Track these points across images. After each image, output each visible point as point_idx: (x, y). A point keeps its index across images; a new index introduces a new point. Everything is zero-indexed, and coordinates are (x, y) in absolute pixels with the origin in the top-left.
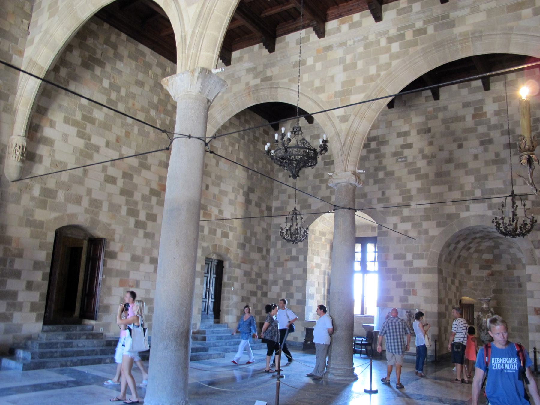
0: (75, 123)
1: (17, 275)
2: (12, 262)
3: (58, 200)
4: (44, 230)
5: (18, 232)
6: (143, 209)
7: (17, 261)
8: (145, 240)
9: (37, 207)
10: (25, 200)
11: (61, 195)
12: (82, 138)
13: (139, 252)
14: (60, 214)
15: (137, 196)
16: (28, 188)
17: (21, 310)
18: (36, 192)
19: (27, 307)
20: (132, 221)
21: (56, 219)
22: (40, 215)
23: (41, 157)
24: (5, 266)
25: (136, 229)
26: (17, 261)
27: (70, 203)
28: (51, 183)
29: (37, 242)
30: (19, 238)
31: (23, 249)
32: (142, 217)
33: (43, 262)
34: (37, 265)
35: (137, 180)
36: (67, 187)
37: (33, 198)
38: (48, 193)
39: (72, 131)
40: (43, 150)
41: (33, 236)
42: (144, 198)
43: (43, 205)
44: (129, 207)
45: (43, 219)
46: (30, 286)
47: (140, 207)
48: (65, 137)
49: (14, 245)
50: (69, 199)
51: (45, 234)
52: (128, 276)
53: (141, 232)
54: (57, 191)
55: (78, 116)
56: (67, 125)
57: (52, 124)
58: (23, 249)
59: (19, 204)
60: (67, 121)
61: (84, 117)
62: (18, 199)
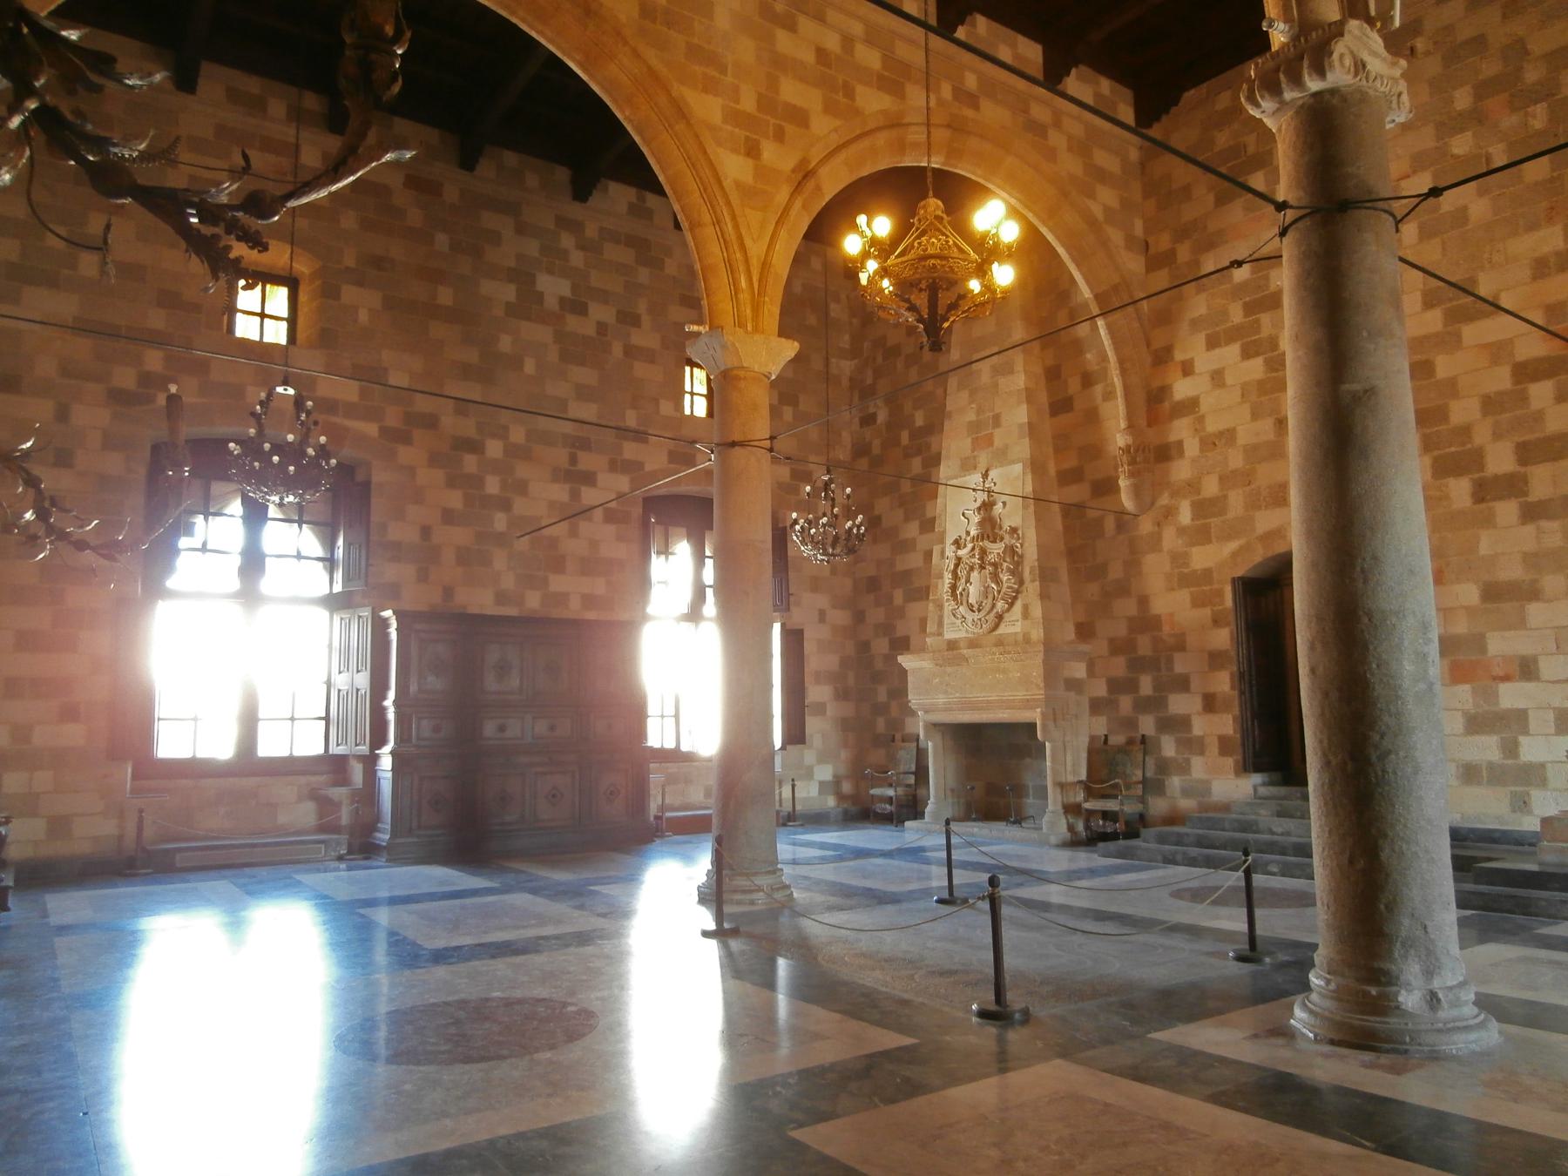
0: (1233, 335)
1: (1183, 684)
2: (1170, 661)
3: (1231, 515)
4: (1216, 586)
5: (1173, 605)
6: (1497, 436)
7: (1177, 656)
8: (1530, 529)
9: (1193, 545)
10: (1170, 539)
11: (1236, 501)
12: (1257, 354)
13: (1511, 571)
14: (1242, 542)
15: (1463, 411)
16: (1170, 513)
17: (1202, 753)
18: (1185, 516)
19: (1213, 748)
20: (1460, 490)
21: (1234, 555)
22: (1203, 557)
23: (1180, 443)
24: (1159, 670)
25: (1483, 506)
26: (1177, 656)
27: (1259, 508)
28: (1211, 488)
29: (1206, 612)
30: (1171, 615)
31: (1183, 634)
32: (1500, 460)
33: (1226, 651)
34: (1215, 659)
35: (1444, 366)
36: (1244, 477)
37: (1182, 531)
38: (1203, 508)
39: (1230, 353)
40: (1181, 430)
41: (1197, 602)
42: (1490, 404)
43: (1201, 535)
44: (1436, 453)
45: (1209, 564)
46: (1210, 704)
47: (1482, 435)
48: (1217, 377)
49: (1166, 629)
50: (1254, 503)
51: (1220, 593)
52: (1483, 649)
53: (1507, 510)
54: (1225, 497)
55: (1237, 315)
56: (1217, 351)
57: (1187, 369)
58: (1183, 634)
59: (1160, 551)
60: (1212, 343)
61: (1250, 309)
62: (1155, 542)
